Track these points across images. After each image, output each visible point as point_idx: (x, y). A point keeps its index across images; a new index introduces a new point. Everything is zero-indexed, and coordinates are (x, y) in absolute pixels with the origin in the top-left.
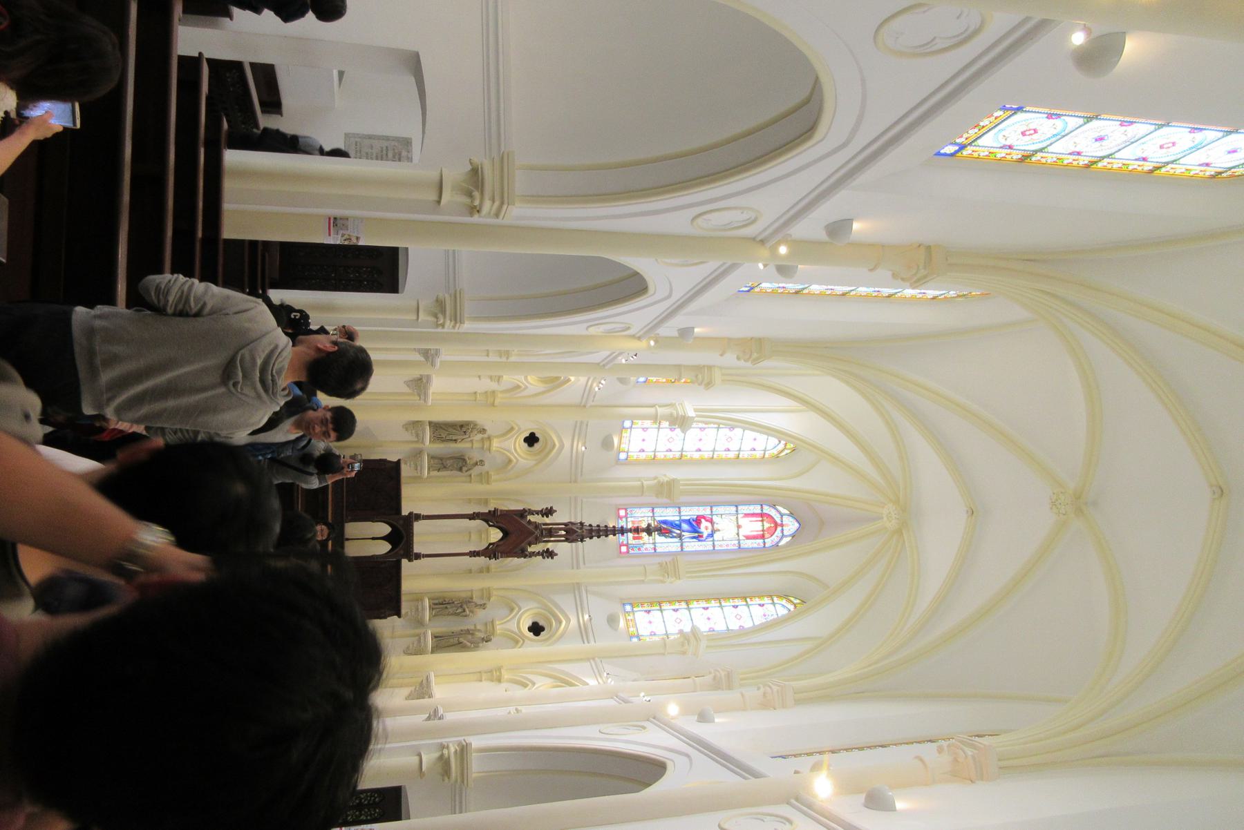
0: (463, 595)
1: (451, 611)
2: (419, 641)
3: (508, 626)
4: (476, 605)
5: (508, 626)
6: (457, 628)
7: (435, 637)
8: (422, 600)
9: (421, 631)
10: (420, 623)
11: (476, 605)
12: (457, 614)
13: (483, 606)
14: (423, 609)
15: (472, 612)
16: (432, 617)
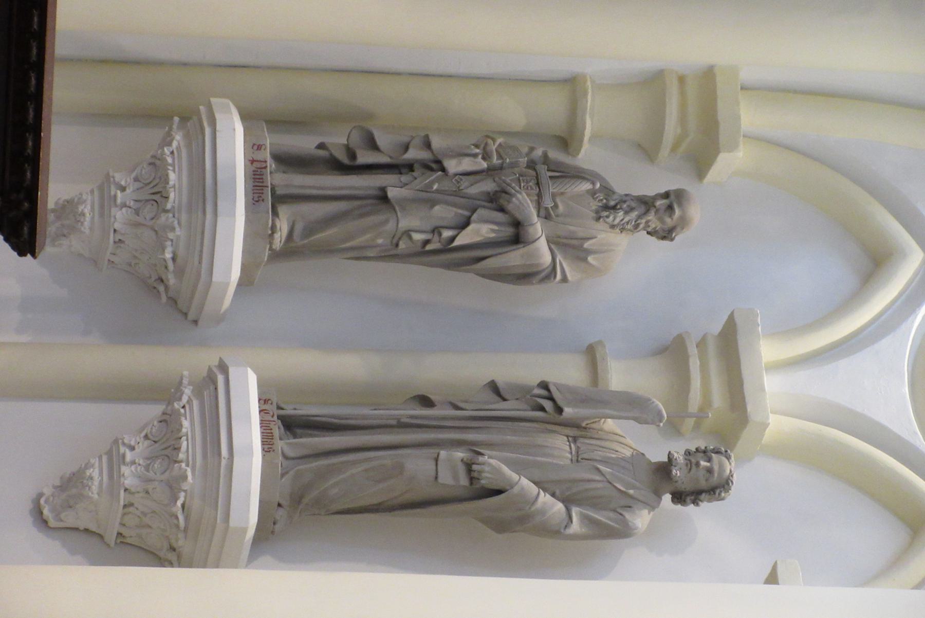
0: (509, 111)
1: (414, 223)
2: (165, 443)
3: (842, 384)
4: (609, 204)
5: (842, 384)
6: (460, 369)
7: (289, 423)
8: (193, 120)
9: (184, 360)
10: (165, 295)
11: (609, 204)
12: (469, 259)
13: (662, 214)
14: (204, 194)
15: (572, 247)
16: (275, 256)
